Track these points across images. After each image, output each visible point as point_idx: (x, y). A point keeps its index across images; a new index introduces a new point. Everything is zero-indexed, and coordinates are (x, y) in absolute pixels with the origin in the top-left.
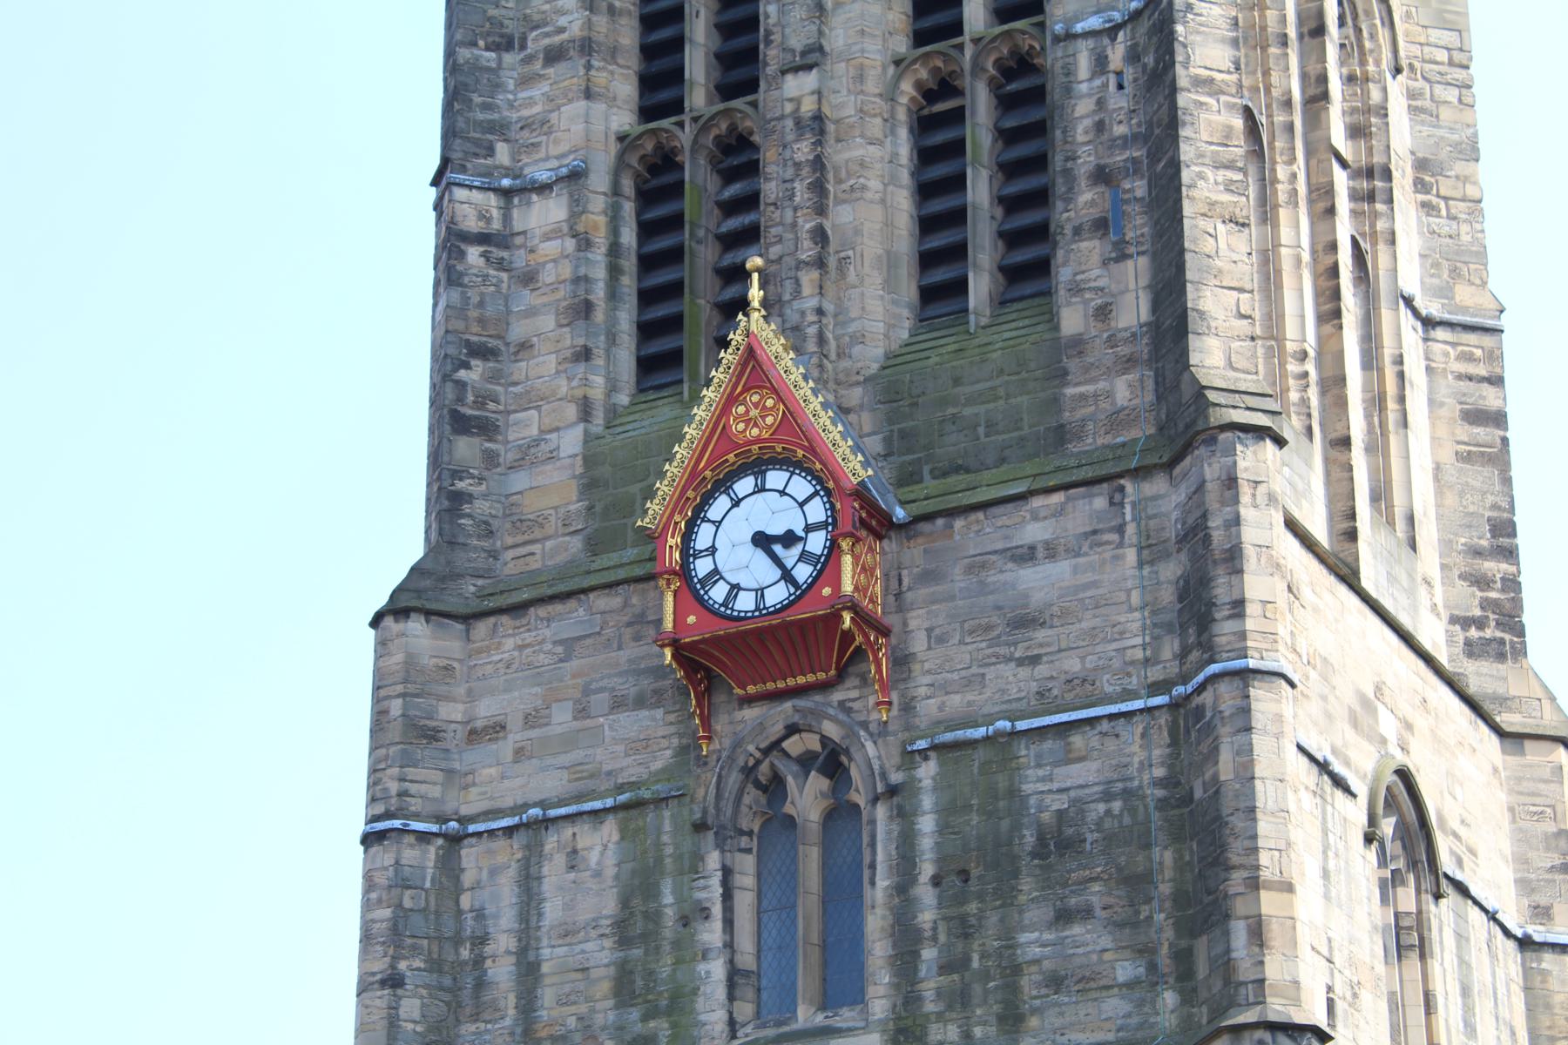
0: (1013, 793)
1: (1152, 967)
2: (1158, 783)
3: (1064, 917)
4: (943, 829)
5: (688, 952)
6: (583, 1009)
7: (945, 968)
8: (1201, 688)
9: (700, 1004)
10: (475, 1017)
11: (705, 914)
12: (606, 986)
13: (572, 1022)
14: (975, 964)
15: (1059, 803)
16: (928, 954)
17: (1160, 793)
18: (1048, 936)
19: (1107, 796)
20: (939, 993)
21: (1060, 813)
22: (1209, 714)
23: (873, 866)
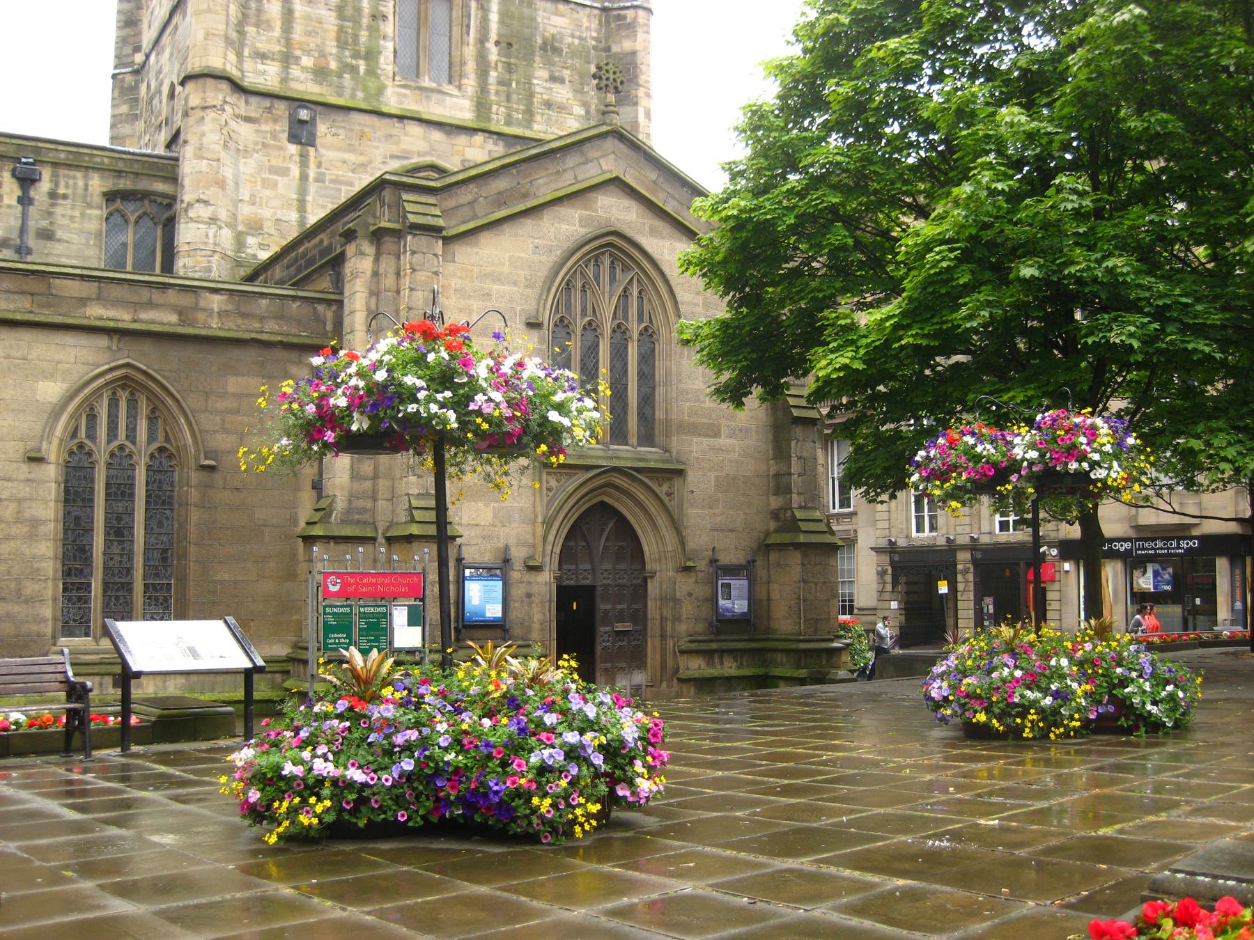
0: (533, 19)
1: (588, 112)
2: (593, 38)
3: (553, 79)
4: (501, 22)
5: (374, 31)
6: (319, 41)
7: (500, 83)
8: (627, 8)
9: (382, 60)
10: (257, 25)
11: (385, 17)
12: (333, 35)
13: (312, 46)
14: (514, 85)
15: (554, 31)
16: (493, 74)
17: (594, 43)
18: (548, 85)
19: (573, 36)
20: (497, 93)
21: (553, 36)
22: (629, 20)
23: (468, 26)
